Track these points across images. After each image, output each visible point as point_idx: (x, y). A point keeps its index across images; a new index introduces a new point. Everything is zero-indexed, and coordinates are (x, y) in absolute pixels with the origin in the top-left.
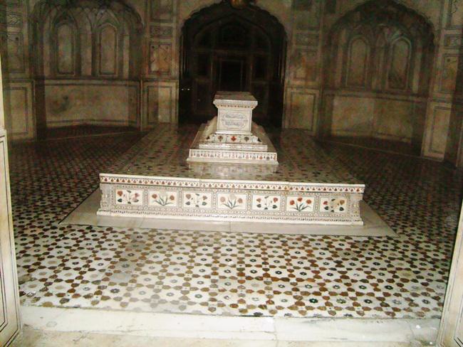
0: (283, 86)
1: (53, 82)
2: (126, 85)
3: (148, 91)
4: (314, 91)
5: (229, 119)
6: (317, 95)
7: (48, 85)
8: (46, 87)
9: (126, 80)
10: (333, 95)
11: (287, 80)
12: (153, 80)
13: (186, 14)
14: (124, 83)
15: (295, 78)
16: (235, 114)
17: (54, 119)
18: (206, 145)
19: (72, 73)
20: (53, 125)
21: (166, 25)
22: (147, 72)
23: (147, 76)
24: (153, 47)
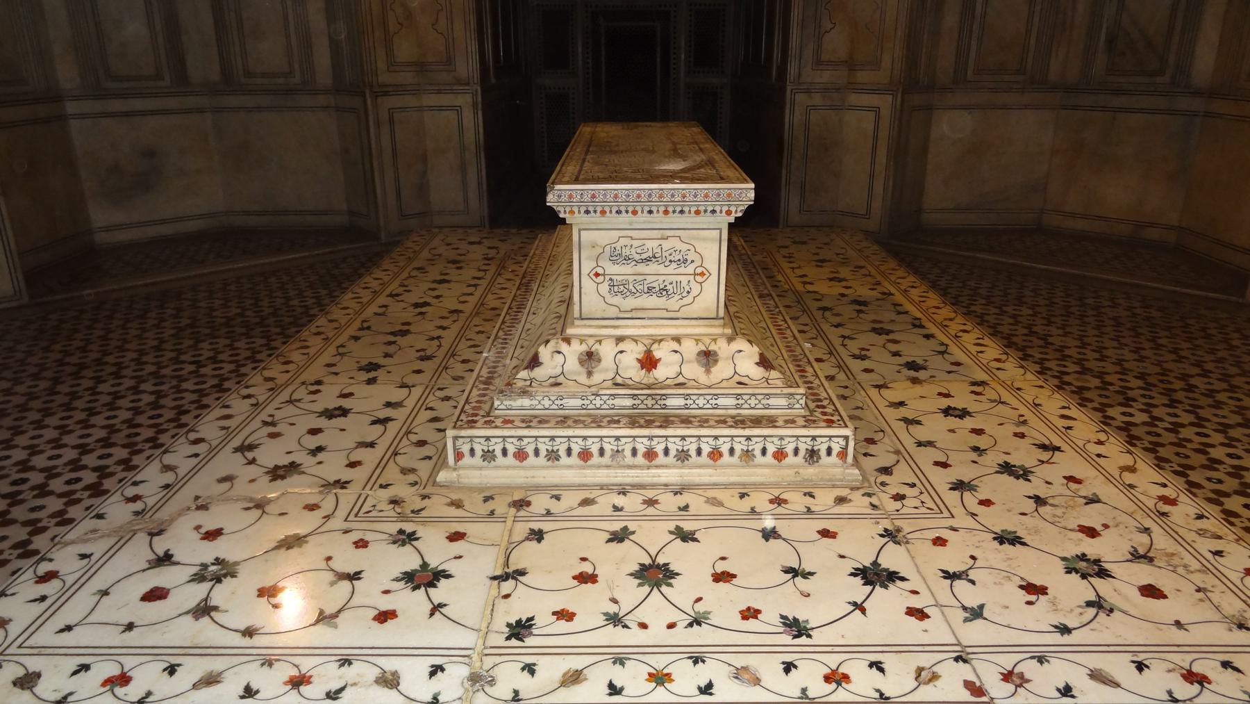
0: (782, 89)
3: (391, 121)
4: (873, 100)
5: (627, 269)
6: (886, 112)
7: (82, 116)
8: (74, 124)
10: (930, 108)
11: (792, 70)
12: (399, 90)
15: (818, 62)
17: (118, 217)
18: (526, 402)
22: (381, 65)
23: (385, 78)
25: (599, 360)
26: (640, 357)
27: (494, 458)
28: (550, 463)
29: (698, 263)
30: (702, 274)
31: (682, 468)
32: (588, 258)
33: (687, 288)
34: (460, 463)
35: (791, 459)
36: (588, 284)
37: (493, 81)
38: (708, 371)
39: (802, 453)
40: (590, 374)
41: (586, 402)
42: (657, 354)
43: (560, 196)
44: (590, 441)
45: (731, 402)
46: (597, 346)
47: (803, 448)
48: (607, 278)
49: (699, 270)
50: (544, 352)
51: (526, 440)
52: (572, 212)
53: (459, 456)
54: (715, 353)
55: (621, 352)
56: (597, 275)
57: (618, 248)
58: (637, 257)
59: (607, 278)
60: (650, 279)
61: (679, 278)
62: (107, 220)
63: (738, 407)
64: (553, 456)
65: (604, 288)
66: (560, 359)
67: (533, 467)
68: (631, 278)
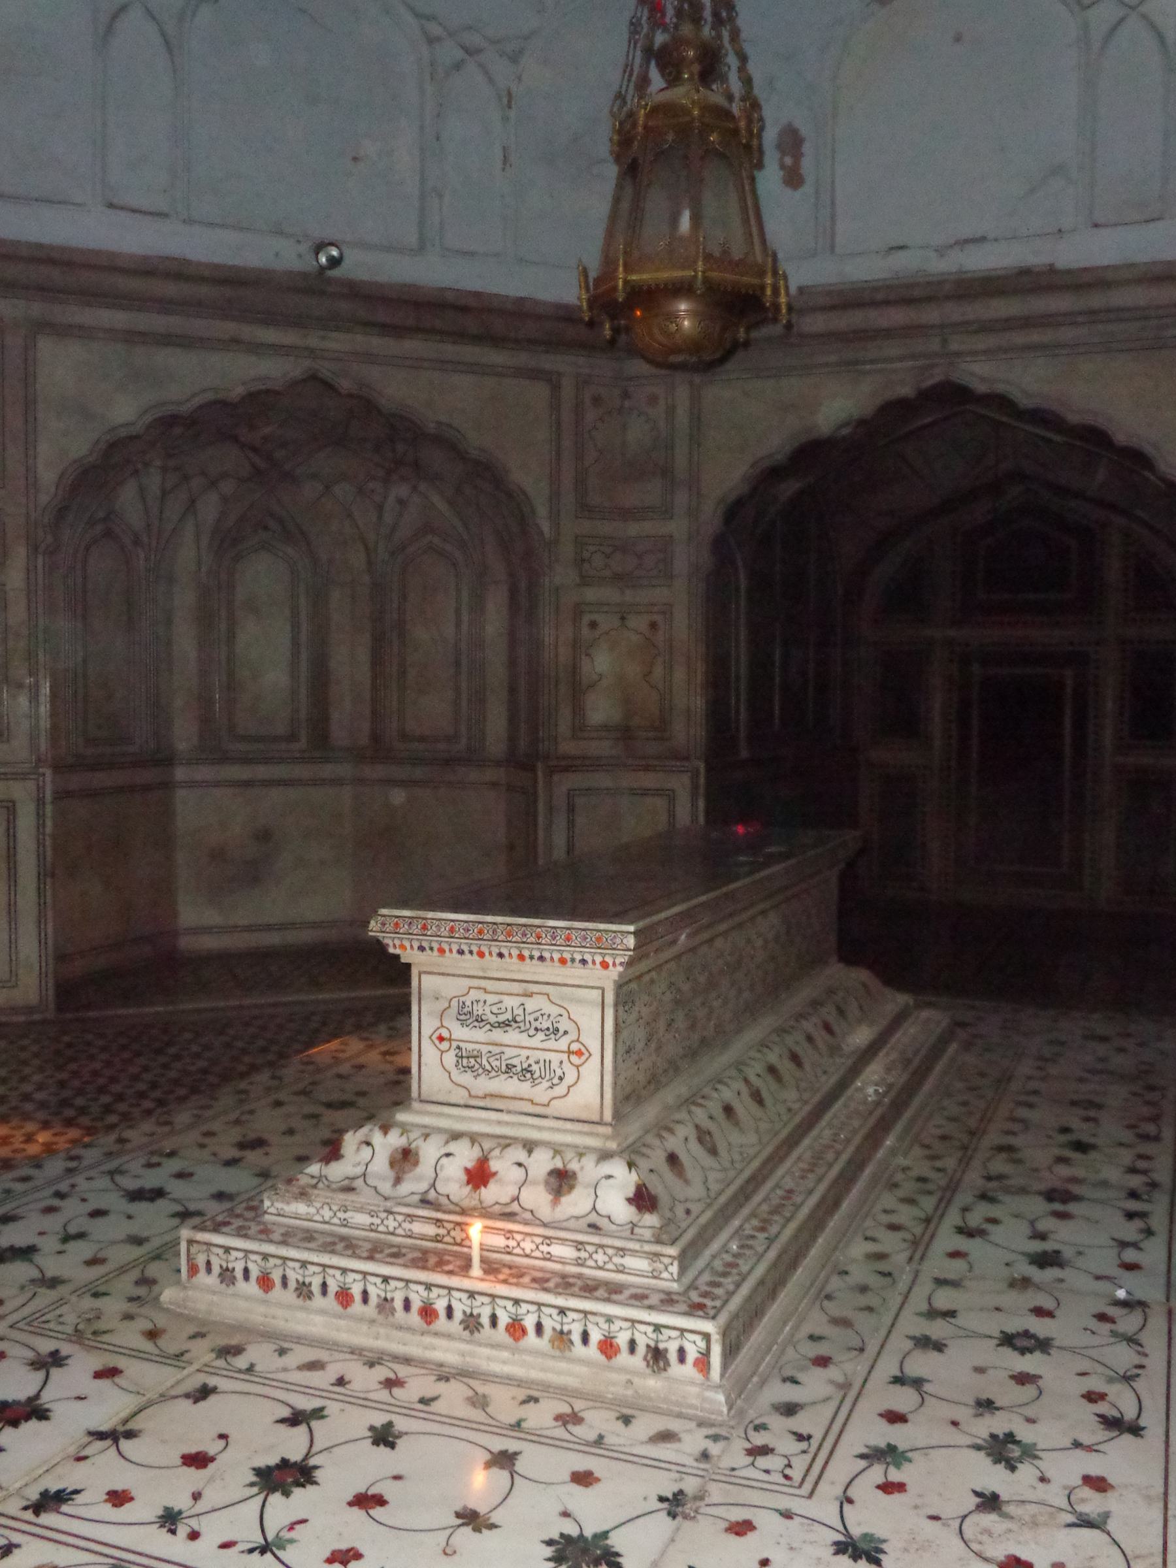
1: (204, 773)
2: (494, 785)
3: (571, 809)
5: (480, 1035)
7: (192, 784)
8: (181, 793)
9: (498, 764)
13: (726, 475)
14: (490, 775)
16: (511, 1002)
17: (211, 917)
18: (301, 1208)
19: (292, 737)
20: (209, 943)
21: (648, 527)
22: (564, 728)
23: (568, 747)
24: (593, 625)
25: (416, 1163)
26: (470, 1165)
27: (233, 1280)
28: (300, 1302)
29: (573, 1036)
30: (579, 1053)
31: (468, 1342)
32: (430, 1014)
33: (559, 1072)
34: (194, 1279)
35: (623, 1358)
36: (430, 1053)
37: (744, 754)
38: (556, 1201)
39: (641, 1349)
40: (398, 1181)
41: (377, 1221)
42: (494, 1165)
43: (383, 924)
44: (351, 1277)
45: (568, 1252)
46: (420, 1142)
47: (642, 1342)
48: (454, 1044)
49: (575, 1047)
50: (350, 1140)
51: (272, 1261)
52: (403, 947)
53: (193, 1270)
54: (574, 1175)
55: (448, 1155)
56: (441, 1039)
57: (468, 1003)
58: (493, 1019)
59: (454, 1044)
60: (509, 1052)
61: (548, 1056)
62: (203, 921)
63: (580, 1262)
64: (304, 1290)
65: (450, 1059)
66: (366, 1152)
67: (280, 1305)
68: (485, 1049)
